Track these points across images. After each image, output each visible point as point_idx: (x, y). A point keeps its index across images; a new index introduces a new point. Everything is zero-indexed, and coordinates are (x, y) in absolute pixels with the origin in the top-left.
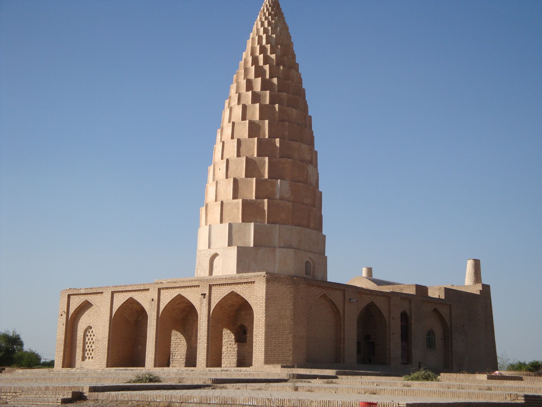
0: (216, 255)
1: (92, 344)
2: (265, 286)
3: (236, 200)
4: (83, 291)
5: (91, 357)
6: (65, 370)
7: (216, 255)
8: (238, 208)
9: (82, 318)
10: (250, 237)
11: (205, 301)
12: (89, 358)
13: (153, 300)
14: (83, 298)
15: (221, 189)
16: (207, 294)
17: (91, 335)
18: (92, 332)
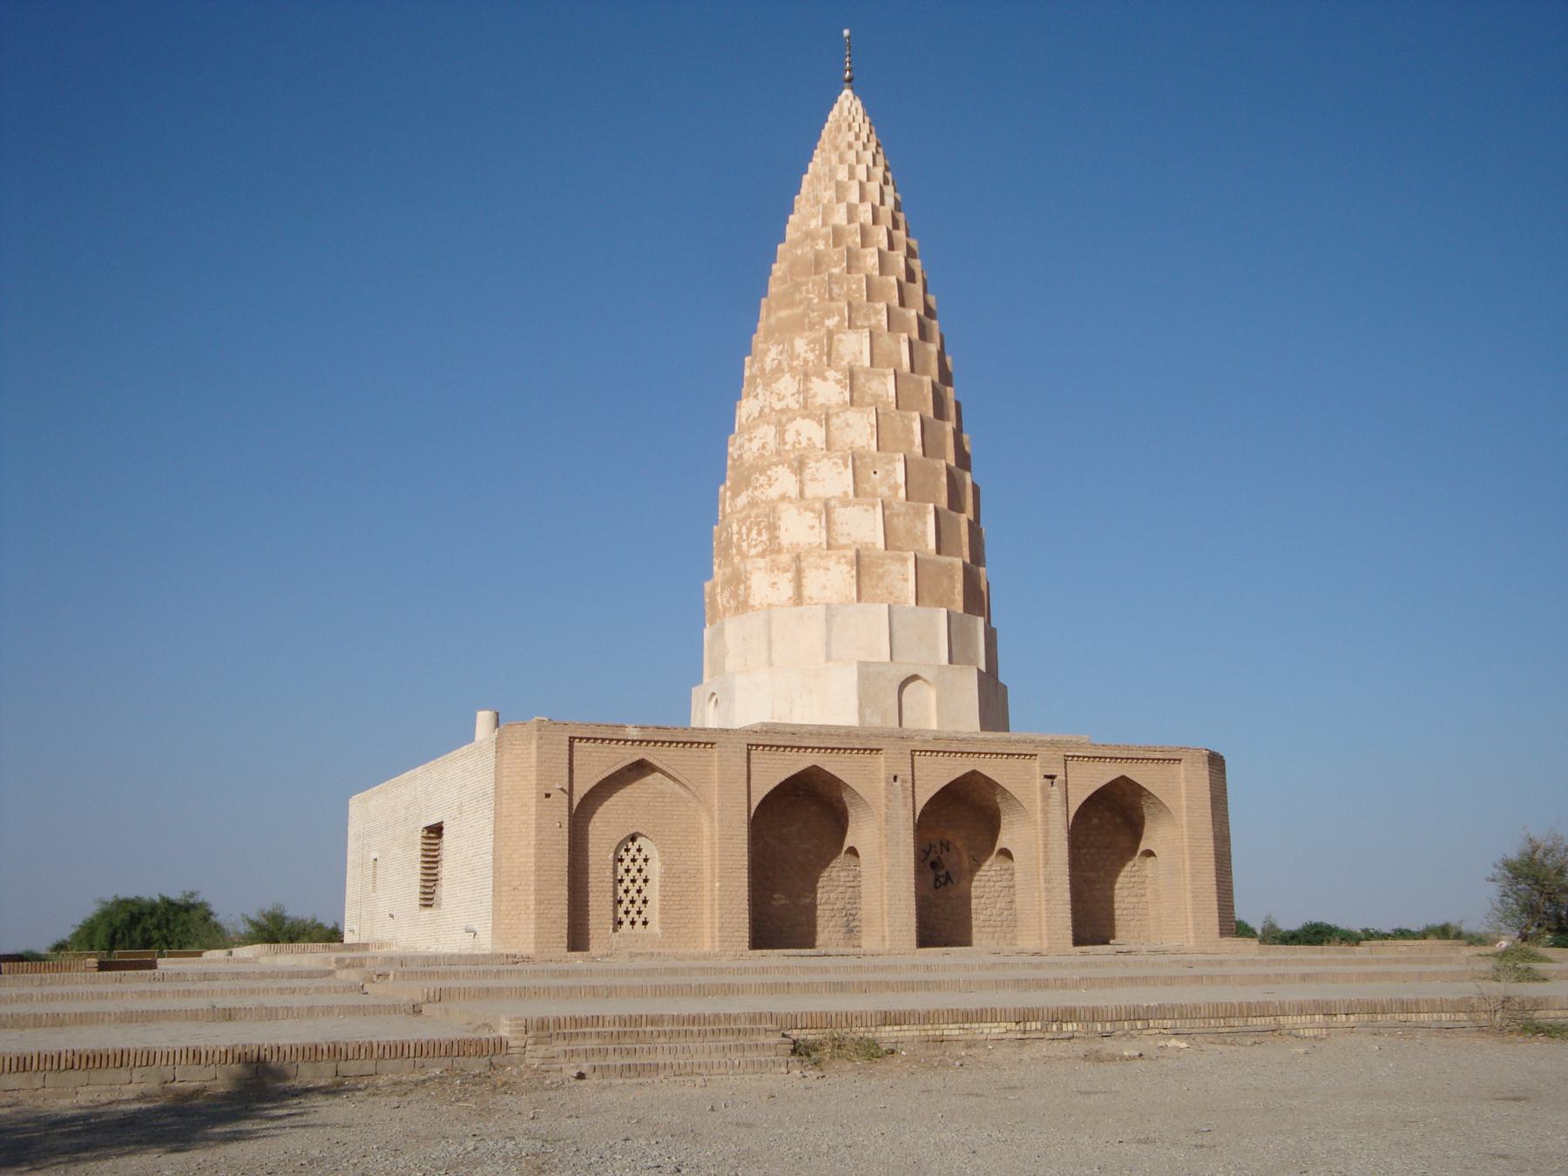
0: (915, 678)
1: (640, 882)
2: (1206, 773)
3: (944, 559)
4: (633, 733)
5: (639, 921)
6: (577, 959)
7: (915, 678)
8: (951, 578)
9: (601, 809)
10: (976, 653)
11: (1056, 791)
12: (633, 923)
13: (895, 778)
14: (630, 755)
15: (899, 523)
16: (1060, 777)
17: (634, 860)
18: (639, 850)
